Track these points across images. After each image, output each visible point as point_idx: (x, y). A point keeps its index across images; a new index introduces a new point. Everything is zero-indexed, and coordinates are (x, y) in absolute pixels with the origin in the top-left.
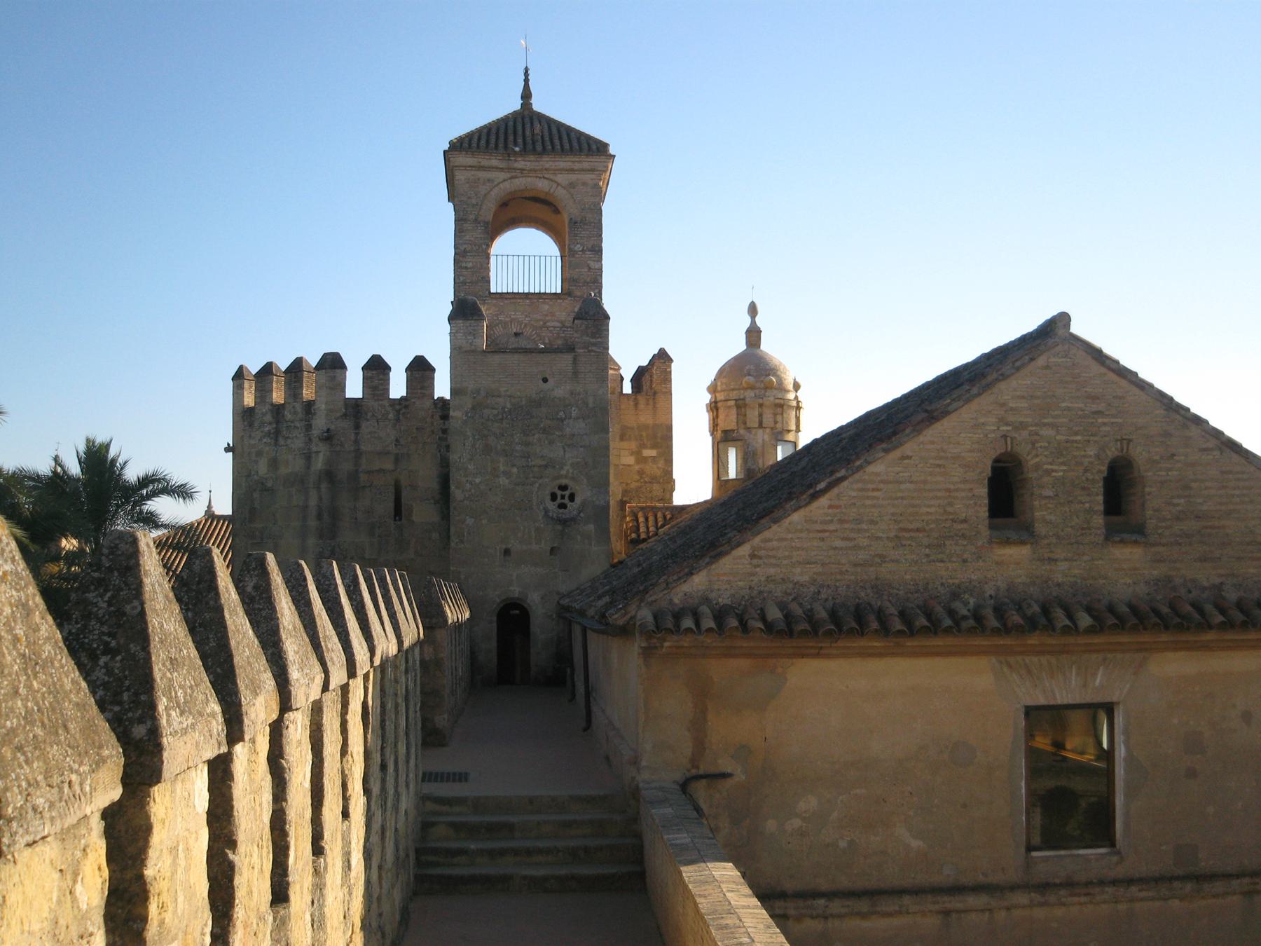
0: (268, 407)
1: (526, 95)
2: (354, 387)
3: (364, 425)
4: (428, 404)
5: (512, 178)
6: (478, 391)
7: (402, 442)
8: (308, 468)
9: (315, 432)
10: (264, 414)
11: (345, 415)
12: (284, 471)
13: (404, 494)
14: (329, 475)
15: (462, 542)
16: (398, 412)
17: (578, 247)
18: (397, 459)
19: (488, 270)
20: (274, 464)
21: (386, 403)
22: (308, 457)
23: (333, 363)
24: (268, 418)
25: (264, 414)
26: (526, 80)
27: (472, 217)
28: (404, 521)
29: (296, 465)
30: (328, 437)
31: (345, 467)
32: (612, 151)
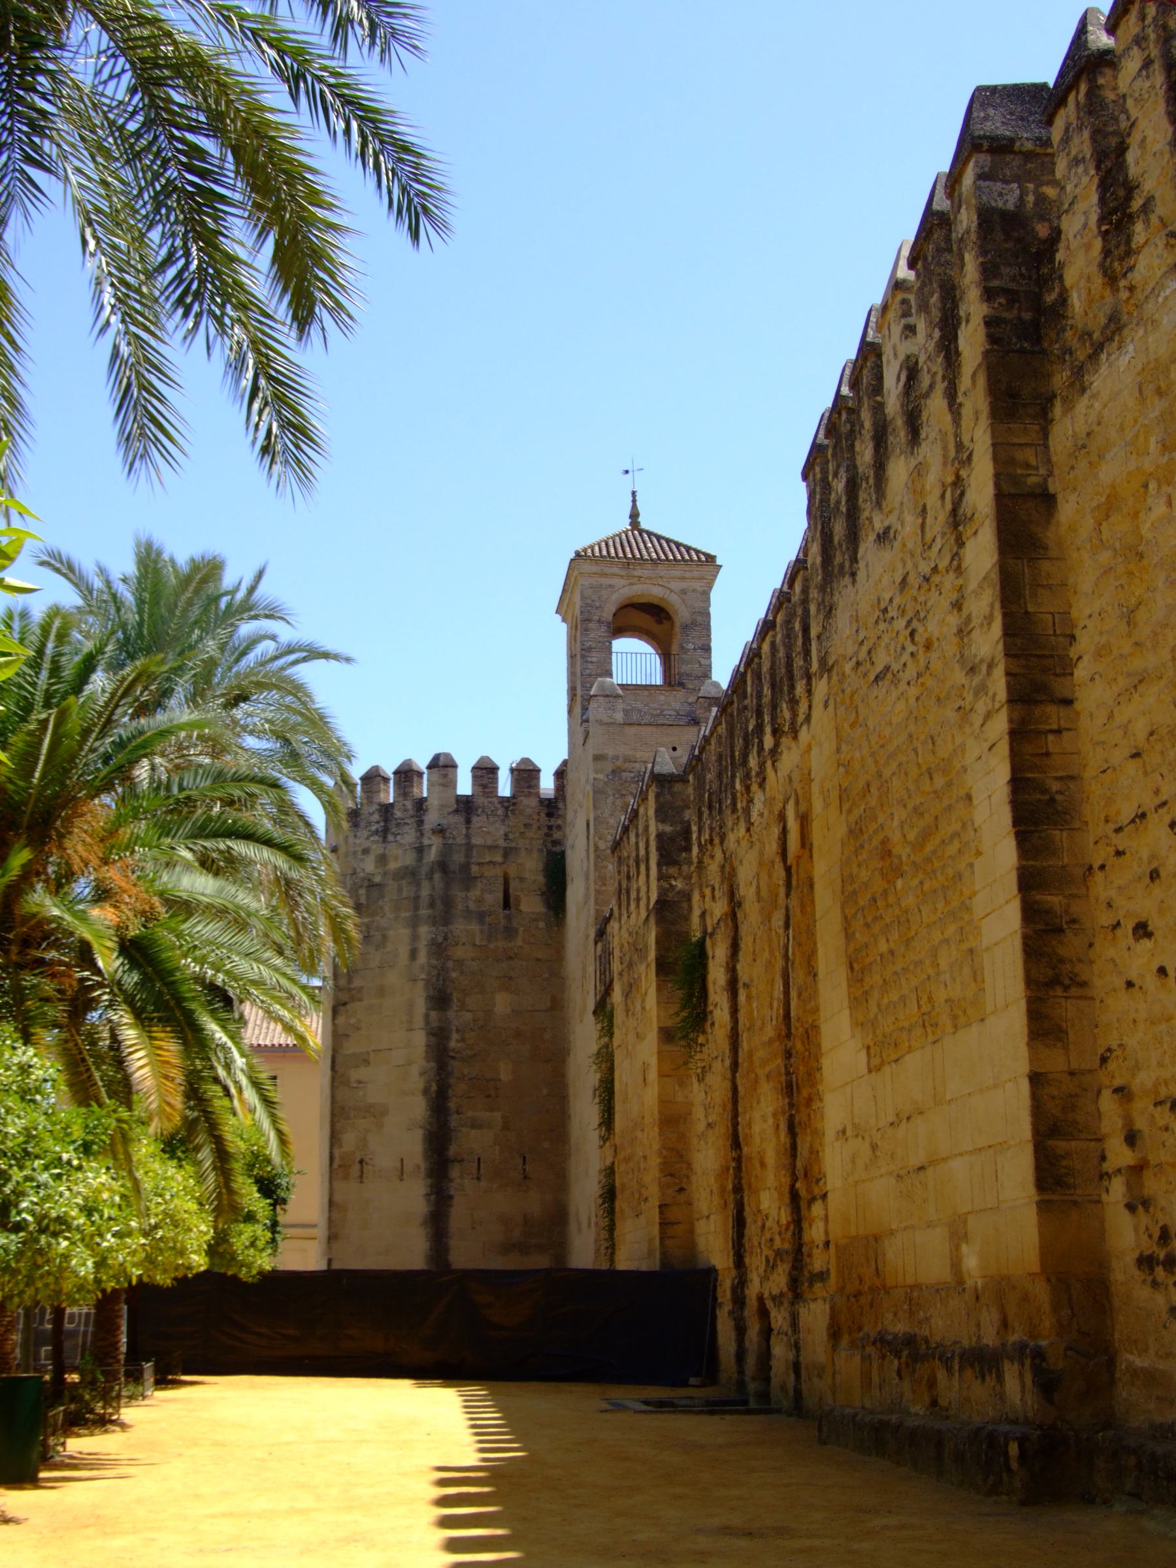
0: (375, 807)
1: (634, 516)
2: (465, 786)
3: (475, 819)
4: (533, 802)
5: (631, 584)
6: (617, 758)
7: (511, 836)
8: (420, 859)
9: (428, 826)
10: (371, 814)
11: (457, 811)
12: (393, 865)
13: (513, 885)
14: (442, 866)
15: (604, 884)
16: (507, 808)
17: (691, 646)
18: (507, 853)
19: (610, 663)
20: (382, 859)
21: (495, 801)
22: (420, 850)
23: (443, 765)
24: (376, 817)
25: (371, 814)
26: (634, 501)
27: (596, 618)
28: (513, 910)
29: (409, 859)
30: (440, 831)
31: (458, 858)
32: (718, 562)
